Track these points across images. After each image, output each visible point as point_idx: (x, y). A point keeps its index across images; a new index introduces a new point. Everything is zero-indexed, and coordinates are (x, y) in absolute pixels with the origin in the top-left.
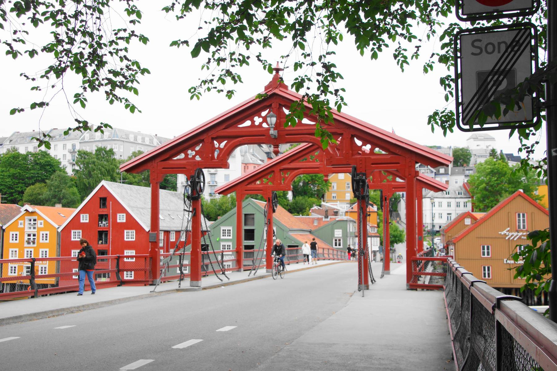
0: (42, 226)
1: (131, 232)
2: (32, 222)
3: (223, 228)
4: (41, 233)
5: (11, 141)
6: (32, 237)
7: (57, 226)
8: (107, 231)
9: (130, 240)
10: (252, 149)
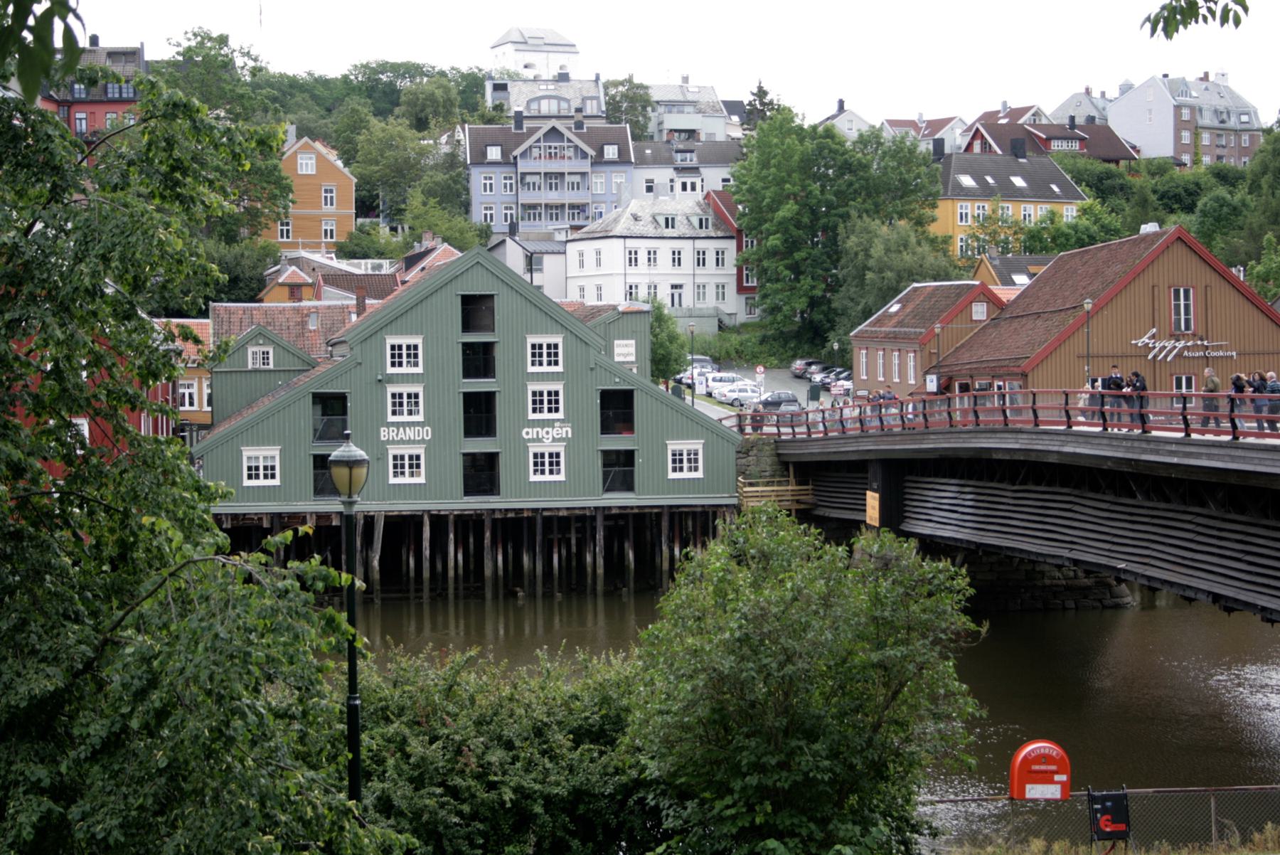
3: (391, 340)
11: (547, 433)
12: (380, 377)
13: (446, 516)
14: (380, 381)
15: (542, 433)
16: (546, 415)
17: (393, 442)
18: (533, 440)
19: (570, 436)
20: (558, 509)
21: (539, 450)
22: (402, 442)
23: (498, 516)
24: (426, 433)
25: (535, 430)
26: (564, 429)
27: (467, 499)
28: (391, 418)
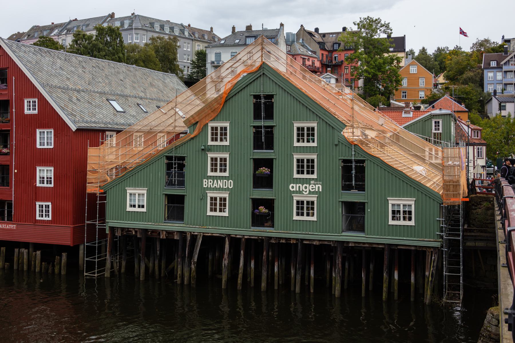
1: (47, 132)
5: (29, 36)
8: (9, 131)
9: (46, 147)
10: (301, 39)
11: (306, 188)
12: (203, 147)
13: (240, 239)
14: (203, 150)
15: (302, 187)
16: (305, 176)
17: (210, 189)
18: (296, 192)
19: (321, 190)
20: (314, 240)
21: (300, 199)
22: (215, 189)
23: (273, 241)
24: (230, 184)
25: (298, 185)
26: (317, 186)
27: (253, 228)
28: (210, 174)
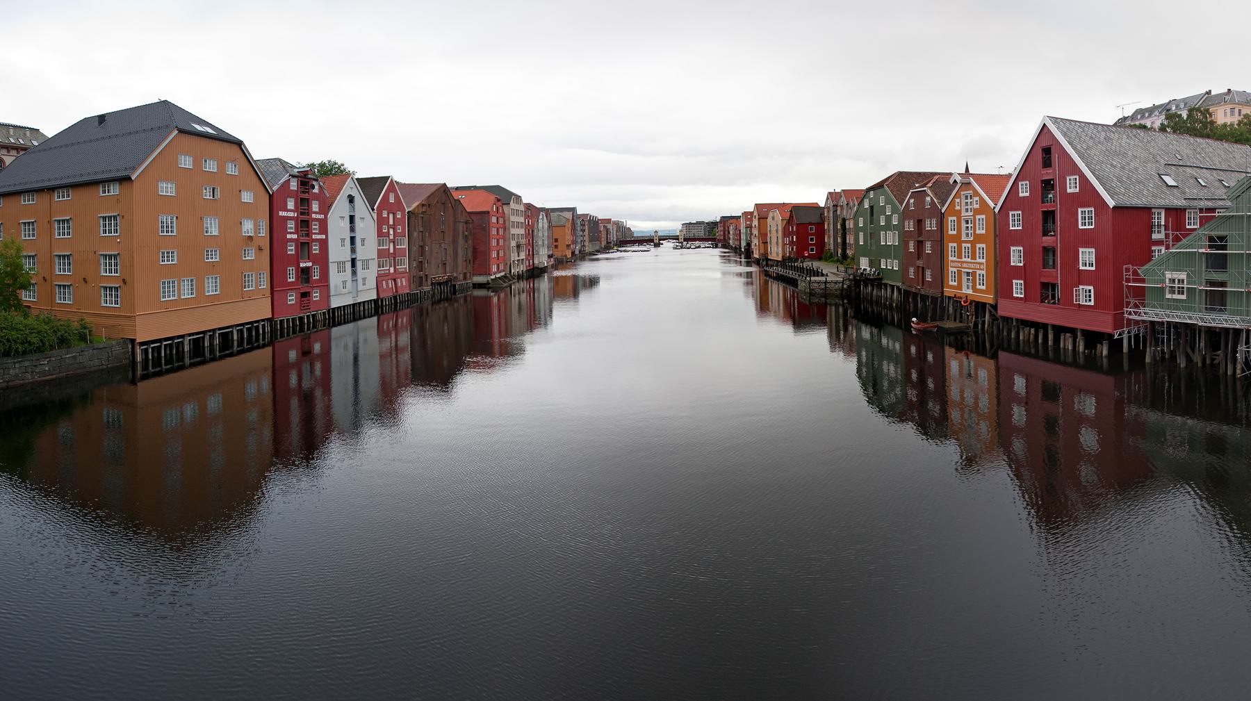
0: (978, 206)
2: (969, 201)
4: (978, 217)
6: (970, 225)
7: (992, 205)
8: (1053, 212)
